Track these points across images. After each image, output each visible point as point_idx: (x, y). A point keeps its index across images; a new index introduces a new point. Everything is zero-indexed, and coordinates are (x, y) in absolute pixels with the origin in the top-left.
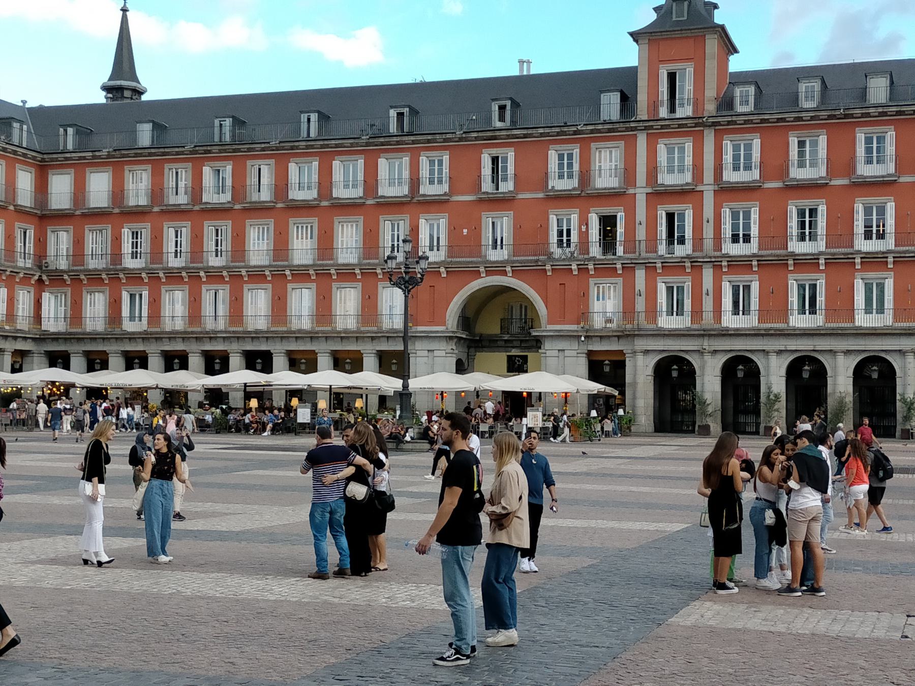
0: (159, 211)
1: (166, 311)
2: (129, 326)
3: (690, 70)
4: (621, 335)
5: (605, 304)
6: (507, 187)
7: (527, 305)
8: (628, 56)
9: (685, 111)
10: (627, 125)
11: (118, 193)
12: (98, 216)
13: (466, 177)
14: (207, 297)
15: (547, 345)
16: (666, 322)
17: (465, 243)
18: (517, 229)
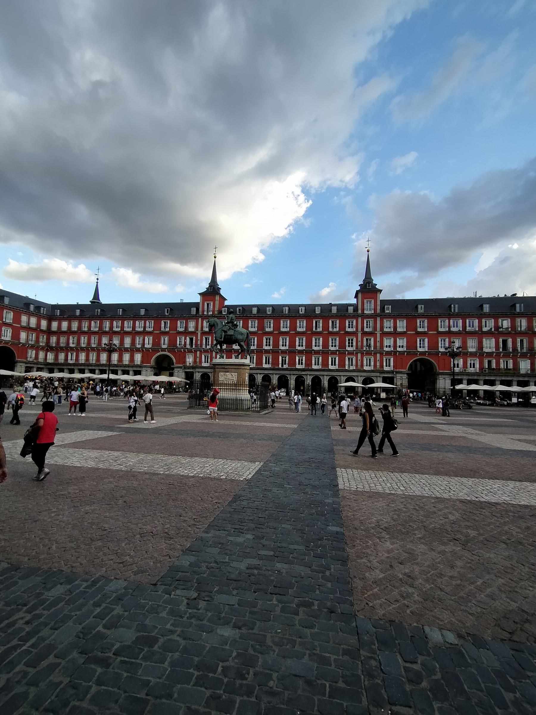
0: (80, 332)
1: (80, 358)
2: (70, 362)
3: (212, 303)
4: (193, 367)
5: (190, 360)
6: (168, 330)
7: (171, 359)
8: (197, 299)
9: (210, 313)
10: (195, 317)
11: (69, 327)
12: (64, 333)
13: (157, 326)
14: (91, 355)
15: (175, 369)
16: (204, 365)
17: (156, 343)
18: (169, 340)
